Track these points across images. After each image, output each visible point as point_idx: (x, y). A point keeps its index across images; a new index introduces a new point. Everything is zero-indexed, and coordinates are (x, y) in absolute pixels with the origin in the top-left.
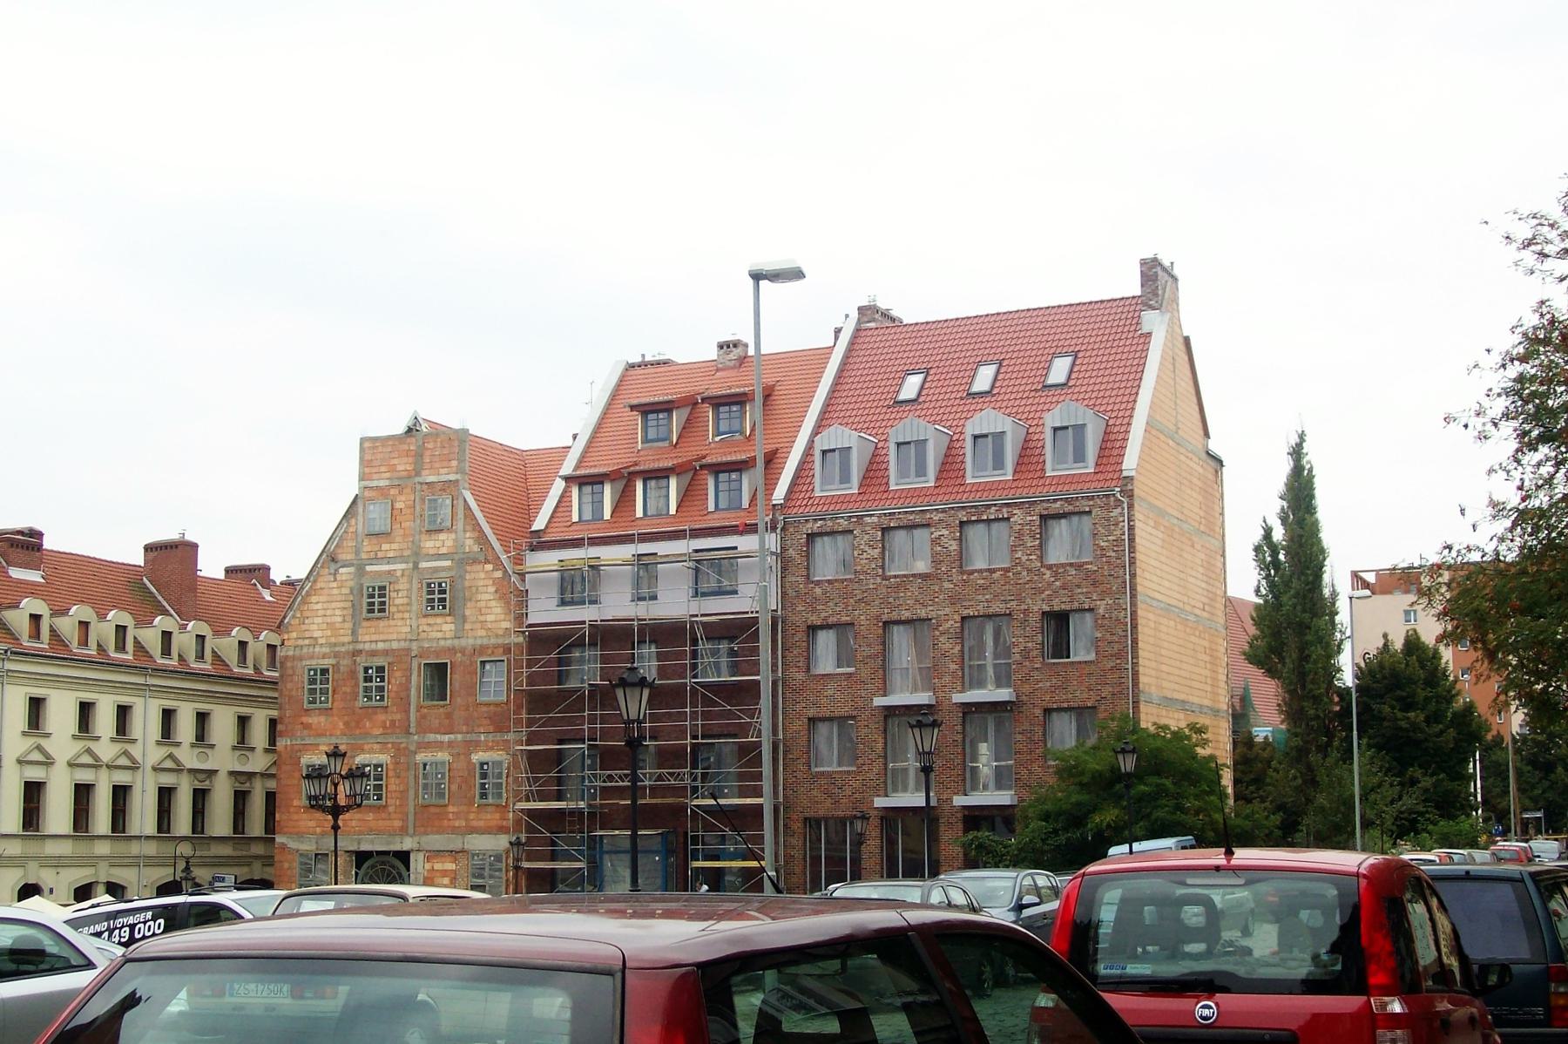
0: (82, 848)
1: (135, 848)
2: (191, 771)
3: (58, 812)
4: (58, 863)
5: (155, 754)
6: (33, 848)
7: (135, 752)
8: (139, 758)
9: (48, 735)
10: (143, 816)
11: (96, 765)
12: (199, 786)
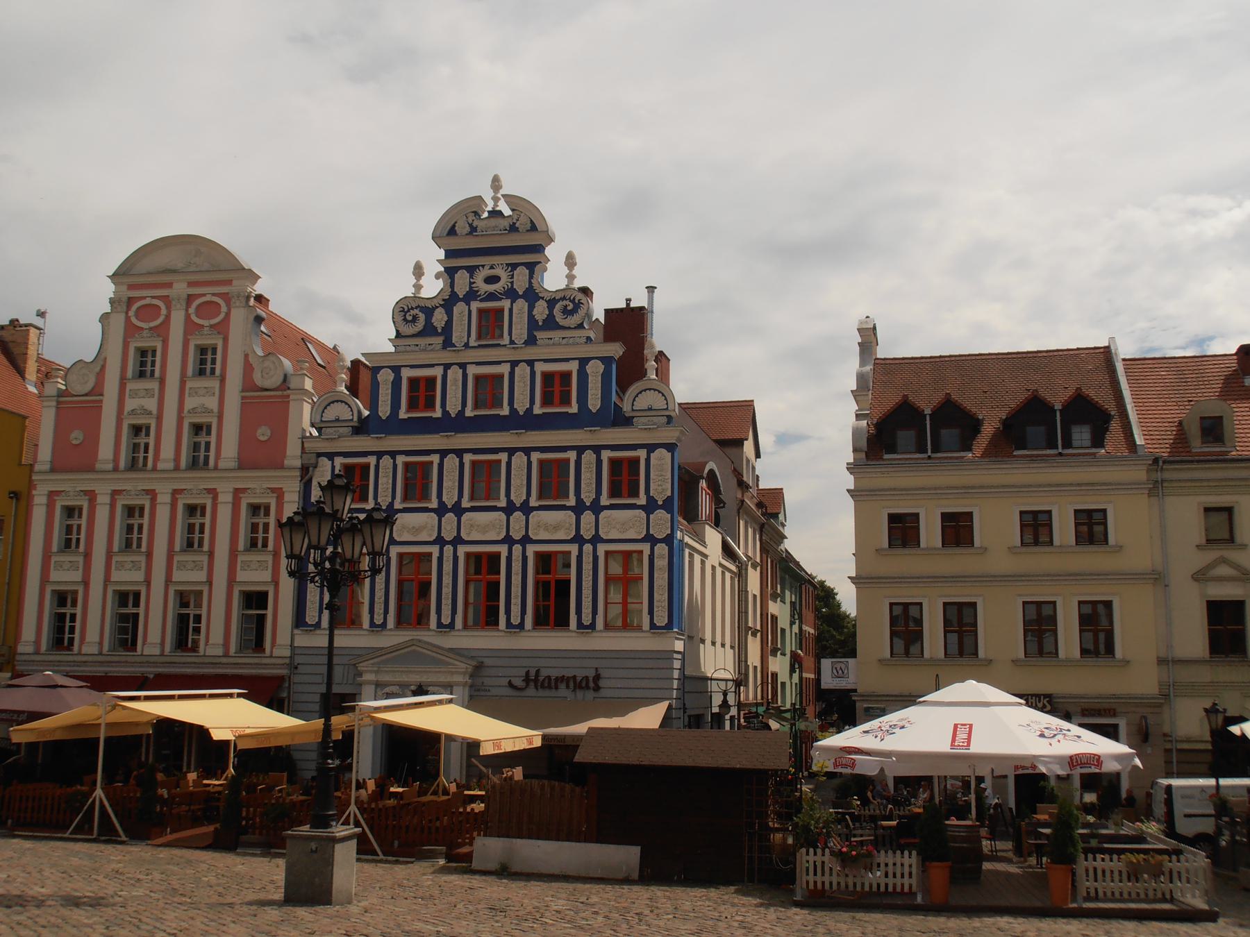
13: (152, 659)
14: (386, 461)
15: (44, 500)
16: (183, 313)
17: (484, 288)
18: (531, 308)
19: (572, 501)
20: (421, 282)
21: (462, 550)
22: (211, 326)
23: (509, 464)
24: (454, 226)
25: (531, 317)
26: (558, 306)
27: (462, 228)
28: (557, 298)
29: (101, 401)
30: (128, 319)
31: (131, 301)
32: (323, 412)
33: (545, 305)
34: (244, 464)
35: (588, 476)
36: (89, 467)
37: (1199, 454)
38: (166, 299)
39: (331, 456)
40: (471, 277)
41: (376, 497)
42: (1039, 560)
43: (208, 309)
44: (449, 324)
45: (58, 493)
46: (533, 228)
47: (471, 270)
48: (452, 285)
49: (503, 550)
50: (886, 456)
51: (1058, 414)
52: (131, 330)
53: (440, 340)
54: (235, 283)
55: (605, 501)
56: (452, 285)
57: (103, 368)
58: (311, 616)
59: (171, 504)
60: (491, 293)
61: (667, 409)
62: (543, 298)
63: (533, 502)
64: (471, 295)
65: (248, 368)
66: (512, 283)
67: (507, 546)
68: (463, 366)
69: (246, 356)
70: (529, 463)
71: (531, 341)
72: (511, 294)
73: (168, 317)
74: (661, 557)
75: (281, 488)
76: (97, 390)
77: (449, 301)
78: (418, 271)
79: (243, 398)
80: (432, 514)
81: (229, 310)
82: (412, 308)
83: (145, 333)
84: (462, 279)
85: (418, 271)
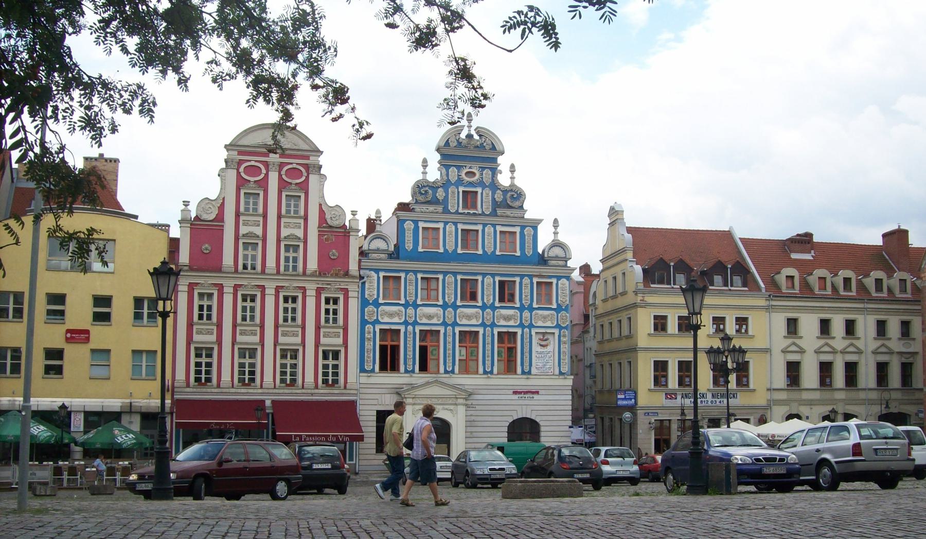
0: (827, 395)
1: (862, 395)
2: (899, 353)
3: (810, 376)
4: (811, 403)
5: (873, 345)
6: (794, 395)
7: (860, 344)
8: (862, 347)
9: (859, 338)
10: (867, 376)
11: (834, 352)
12: (904, 360)
13: (271, 391)
14: (411, 276)
15: (186, 288)
16: (277, 174)
17: (467, 179)
19: (518, 305)
20: (427, 169)
21: (457, 329)
22: (255, 182)
23: (483, 282)
24: (448, 140)
25: (493, 199)
26: (509, 194)
27: (453, 144)
29: (223, 226)
30: (238, 173)
31: (240, 162)
32: (369, 244)
33: (501, 193)
34: (322, 272)
35: (526, 291)
36: (218, 268)
37: (784, 293)
38: (266, 165)
39: (377, 271)
40: (458, 172)
41: (405, 297)
42: (661, 342)
43: (294, 173)
44: (446, 197)
45: (240, 286)
46: (494, 148)
47: (459, 168)
48: (447, 175)
50: (652, 286)
51: (729, 269)
52: (241, 183)
53: (440, 209)
54: (311, 158)
55: (535, 306)
56: (447, 175)
57: (223, 204)
58: (368, 367)
59: (234, 294)
61: (565, 257)
62: (500, 189)
63: (459, 303)
64: (460, 182)
65: (322, 213)
66: (482, 178)
67: (404, 326)
68: (455, 224)
69: (320, 205)
70: (494, 282)
71: (494, 214)
72: (481, 184)
73: (267, 175)
74: (564, 336)
75: (222, 284)
76: (220, 217)
77: (446, 184)
78: (425, 164)
79: (319, 231)
80: (440, 308)
81: (308, 175)
82: (424, 186)
83: (252, 185)
84: (453, 172)
85: (425, 164)
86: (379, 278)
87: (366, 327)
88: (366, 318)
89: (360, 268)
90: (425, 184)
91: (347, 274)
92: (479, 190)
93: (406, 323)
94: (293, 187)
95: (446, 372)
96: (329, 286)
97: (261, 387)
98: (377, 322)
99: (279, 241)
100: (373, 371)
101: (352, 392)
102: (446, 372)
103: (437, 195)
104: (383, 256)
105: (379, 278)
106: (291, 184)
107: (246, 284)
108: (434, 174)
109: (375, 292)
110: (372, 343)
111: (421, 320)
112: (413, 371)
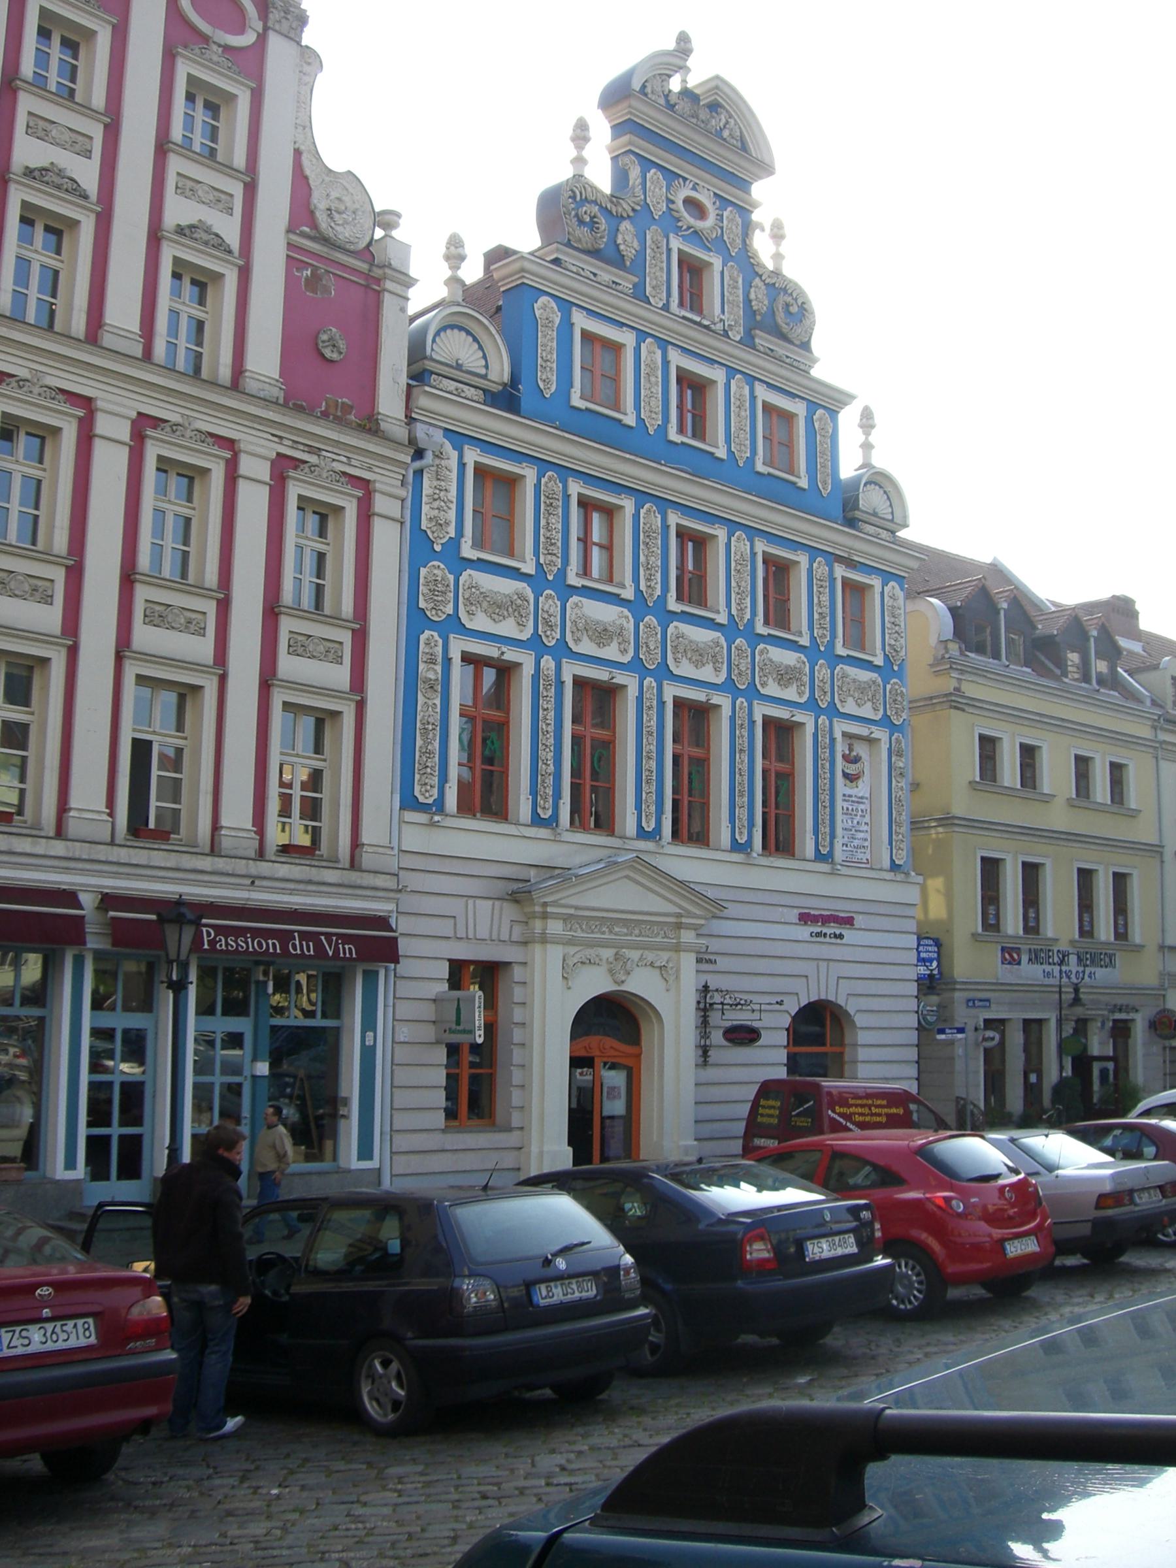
13: (102, 852)
18: (748, 285)
20: (586, 153)
28: (777, 285)
39: (458, 439)
49: (722, 700)
60: (696, 232)
65: (301, 182)
69: (298, 153)
79: (290, 246)
85: (581, 135)
86: (462, 466)
87: (423, 638)
88: (422, 604)
89: (410, 420)
90: (591, 197)
91: (370, 425)
92: (716, 262)
93: (536, 644)
94: (215, 52)
95: (642, 834)
96: (313, 459)
97: (60, 833)
98: (454, 624)
99: (155, 238)
100: (439, 806)
101: (380, 881)
102: (642, 834)
103: (619, 241)
104: (470, 392)
105: (462, 466)
106: (205, 39)
107: (22, 373)
108: (601, 177)
109: (452, 515)
110: (438, 702)
111: (577, 641)
112: (554, 820)
